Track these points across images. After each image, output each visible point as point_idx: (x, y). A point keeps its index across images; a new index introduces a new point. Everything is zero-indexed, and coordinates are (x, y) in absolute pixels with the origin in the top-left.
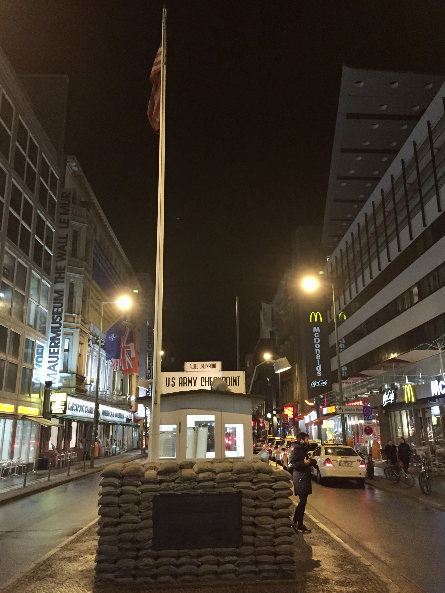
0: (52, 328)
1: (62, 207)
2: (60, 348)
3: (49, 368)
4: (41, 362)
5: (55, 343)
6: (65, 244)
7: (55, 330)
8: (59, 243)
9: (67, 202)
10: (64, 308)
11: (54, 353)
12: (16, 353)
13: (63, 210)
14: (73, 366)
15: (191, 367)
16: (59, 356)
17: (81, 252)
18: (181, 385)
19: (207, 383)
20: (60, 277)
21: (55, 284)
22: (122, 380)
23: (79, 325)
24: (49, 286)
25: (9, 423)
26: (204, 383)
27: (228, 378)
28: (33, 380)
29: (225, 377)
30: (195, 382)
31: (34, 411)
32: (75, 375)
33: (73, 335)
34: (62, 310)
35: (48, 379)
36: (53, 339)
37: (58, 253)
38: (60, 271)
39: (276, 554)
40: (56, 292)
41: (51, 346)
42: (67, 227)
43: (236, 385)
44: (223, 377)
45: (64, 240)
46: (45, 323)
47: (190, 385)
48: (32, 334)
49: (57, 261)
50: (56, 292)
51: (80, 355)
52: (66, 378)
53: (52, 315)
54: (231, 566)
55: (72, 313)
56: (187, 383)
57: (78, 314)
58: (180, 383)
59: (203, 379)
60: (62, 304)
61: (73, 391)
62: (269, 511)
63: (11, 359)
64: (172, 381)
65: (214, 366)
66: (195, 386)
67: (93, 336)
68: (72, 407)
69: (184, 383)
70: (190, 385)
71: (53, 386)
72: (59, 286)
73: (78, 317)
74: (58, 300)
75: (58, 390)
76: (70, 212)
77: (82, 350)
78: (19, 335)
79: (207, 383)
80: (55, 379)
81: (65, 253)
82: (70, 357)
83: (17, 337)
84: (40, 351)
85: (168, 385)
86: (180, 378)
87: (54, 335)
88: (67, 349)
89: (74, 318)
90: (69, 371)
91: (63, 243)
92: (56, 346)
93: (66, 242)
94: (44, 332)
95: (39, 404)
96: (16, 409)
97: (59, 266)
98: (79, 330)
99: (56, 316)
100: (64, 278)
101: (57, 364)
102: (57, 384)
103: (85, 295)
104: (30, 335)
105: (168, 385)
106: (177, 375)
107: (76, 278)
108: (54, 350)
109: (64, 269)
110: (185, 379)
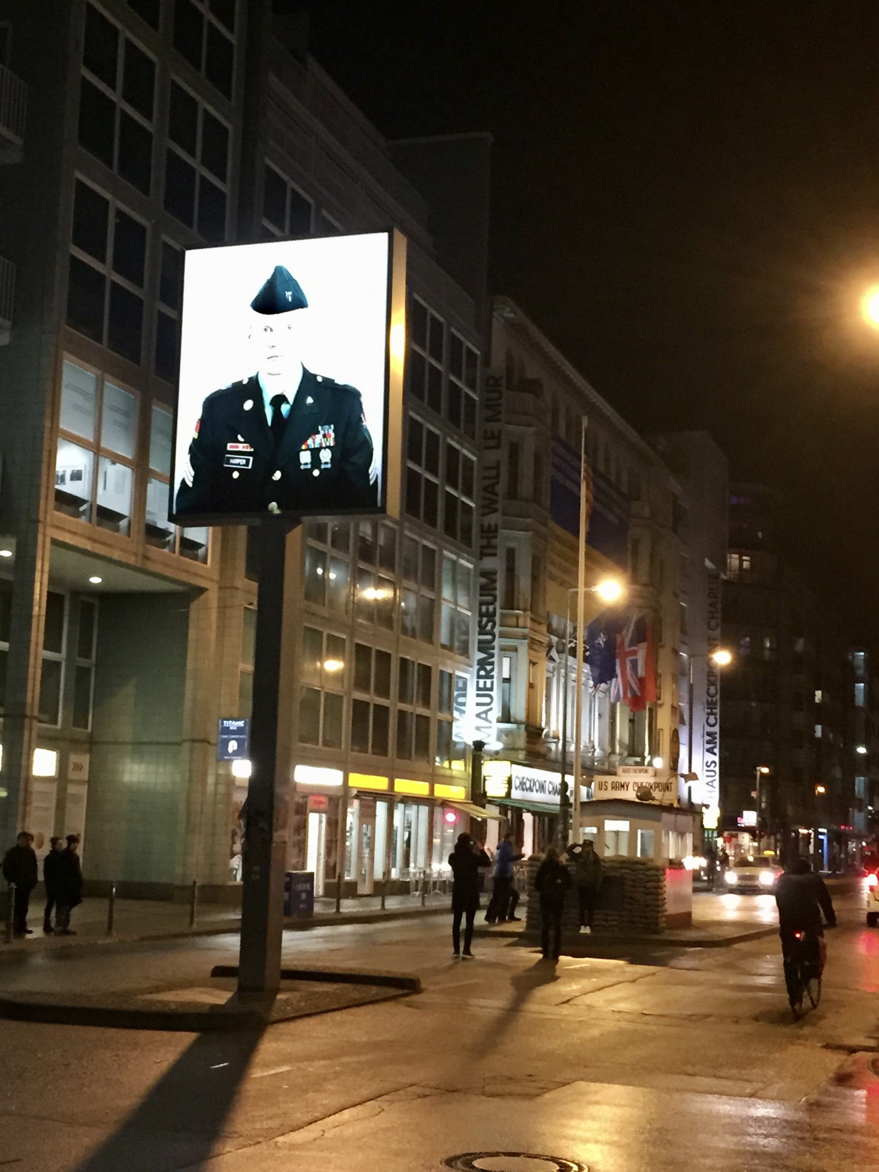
0: (480, 642)
1: (488, 407)
2: (495, 680)
3: (478, 715)
4: (464, 704)
5: (485, 670)
6: (495, 481)
7: (485, 647)
8: (485, 478)
9: (496, 395)
10: (498, 604)
11: (485, 689)
12: (426, 703)
13: (490, 413)
14: (519, 710)
16: (494, 694)
17: (526, 487)
20: (489, 546)
21: (481, 559)
22: (631, 721)
23: (526, 631)
24: (471, 566)
25: (424, 810)
28: (454, 738)
31: (457, 793)
32: (523, 727)
33: (516, 650)
34: (495, 609)
35: (478, 737)
36: (482, 663)
37: (484, 498)
38: (489, 532)
39: (646, 918)
40: (484, 574)
41: (479, 677)
42: (498, 447)
45: (493, 473)
46: (467, 633)
48: (448, 662)
49: (483, 515)
50: (484, 574)
51: (531, 686)
52: (508, 733)
53: (477, 619)
54: (615, 923)
55: (513, 609)
57: (525, 610)
60: (495, 597)
61: (522, 755)
62: (643, 889)
63: (421, 711)
67: (557, 636)
68: (522, 784)
71: (486, 747)
72: (489, 563)
73: (525, 616)
74: (487, 589)
75: (496, 756)
76: (501, 416)
77: (535, 677)
78: (430, 668)
80: (489, 736)
81: (494, 497)
82: (513, 693)
83: (426, 671)
84: (460, 685)
87: (483, 655)
88: (507, 677)
89: (517, 617)
90: (512, 720)
91: (493, 478)
92: (488, 676)
93: (497, 477)
94: (465, 651)
95: (465, 780)
96: (432, 790)
97: (486, 523)
98: (526, 641)
99: (485, 620)
100: (495, 547)
101: (491, 709)
102: (493, 745)
103: (537, 563)
104: (444, 664)
106: (610, 779)
107: (516, 538)
108: (485, 683)
109: (496, 531)
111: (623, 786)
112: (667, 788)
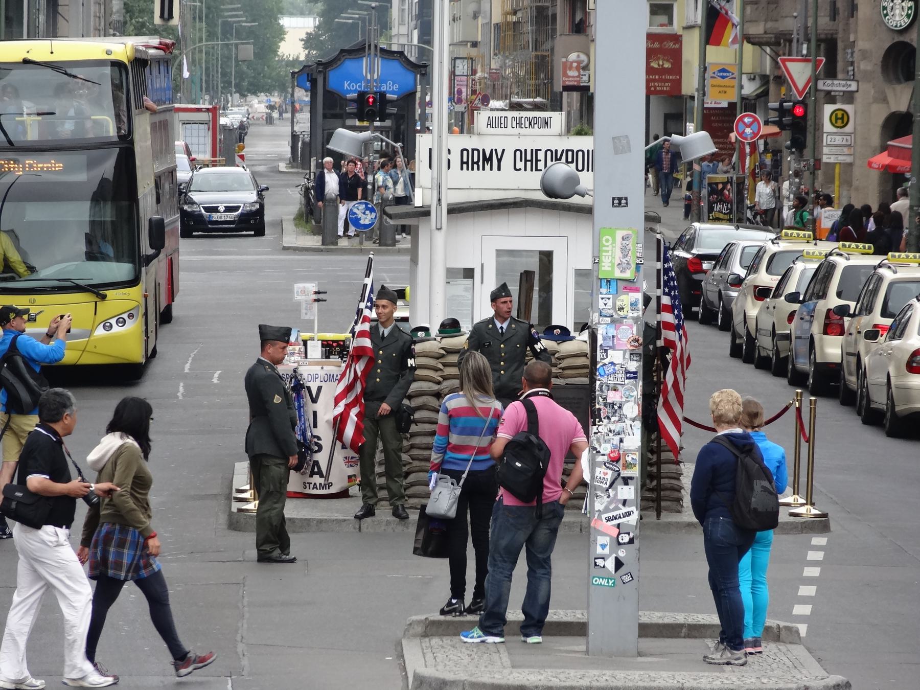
15: (490, 124)
18: (465, 166)
19: (529, 164)
26: (520, 165)
27: (580, 154)
29: (573, 151)
30: (499, 161)
44: (567, 151)
47: (487, 167)
56: (481, 163)
58: (462, 163)
59: (518, 153)
65: (546, 123)
66: (499, 169)
69: (473, 163)
70: (487, 167)
79: (529, 164)
86: (462, 151)
110: (476, 152)
111: (488, 159)
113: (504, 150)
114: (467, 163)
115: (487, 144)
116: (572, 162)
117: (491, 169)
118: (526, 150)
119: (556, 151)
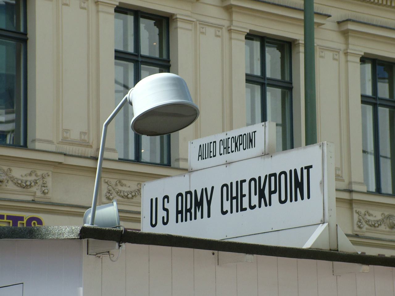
18: (180, 215)
27: (283, 176)
30: (209, 203)
43: (302, 198)
44: (271, 175)
47: (199, 214)
56: (193, 211)
58: (178, 212)
64: (165, 209)
65: (251, 141)
70: (199, 214)
79: (234, 201)
85: (154, 223)
105: (154, 223)
112: (299, 185)
113: (213, 188)
114: (181, 212)
115: (195, 183)
116: (275, 192)
117: (202, 217)
118: (231, 183)
119: (260, 178)
